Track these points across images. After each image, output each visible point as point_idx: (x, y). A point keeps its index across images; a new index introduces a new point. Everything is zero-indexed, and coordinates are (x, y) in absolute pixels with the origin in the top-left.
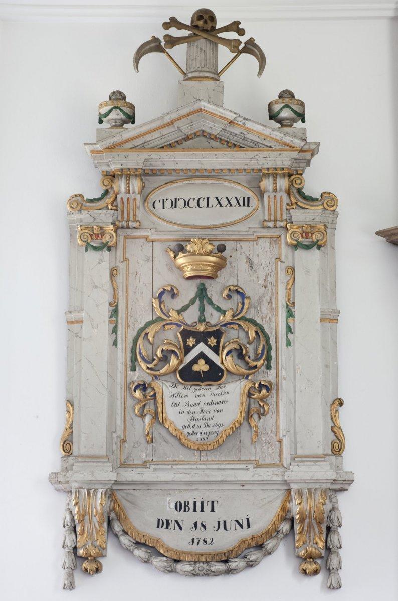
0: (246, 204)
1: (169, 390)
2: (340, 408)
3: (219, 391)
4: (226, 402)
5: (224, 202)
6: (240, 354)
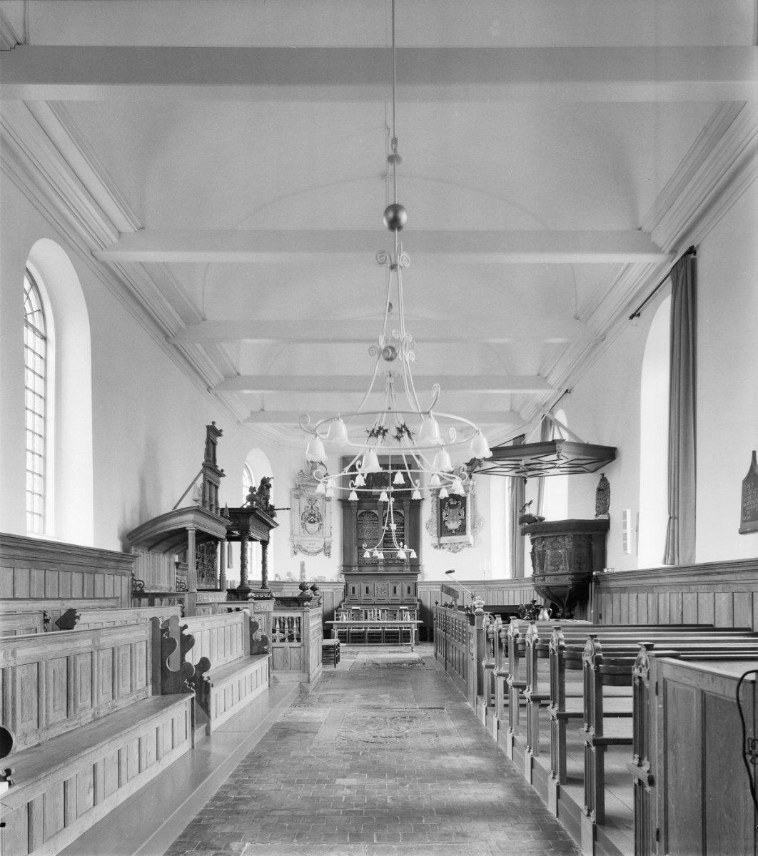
1: (307, 524)
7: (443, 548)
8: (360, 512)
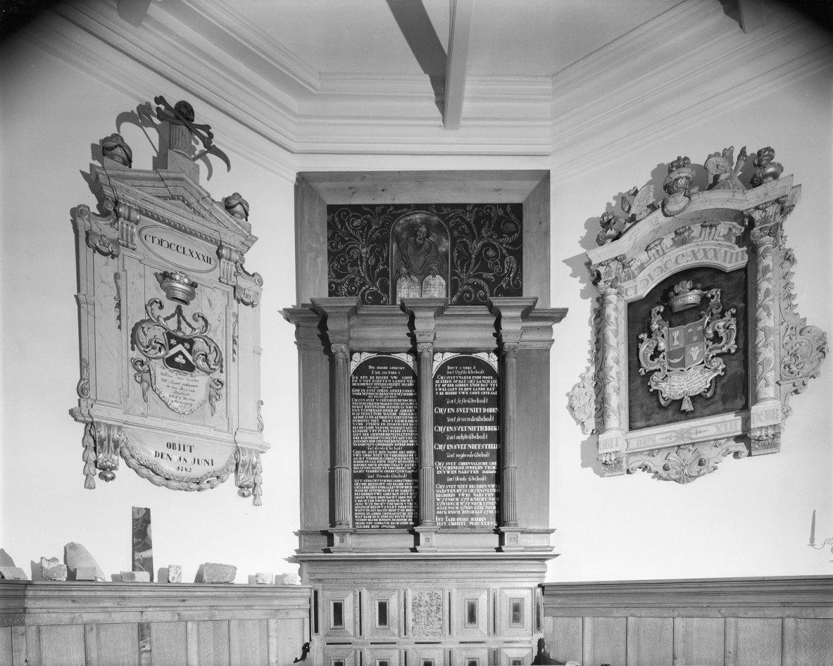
3: (192, 378)
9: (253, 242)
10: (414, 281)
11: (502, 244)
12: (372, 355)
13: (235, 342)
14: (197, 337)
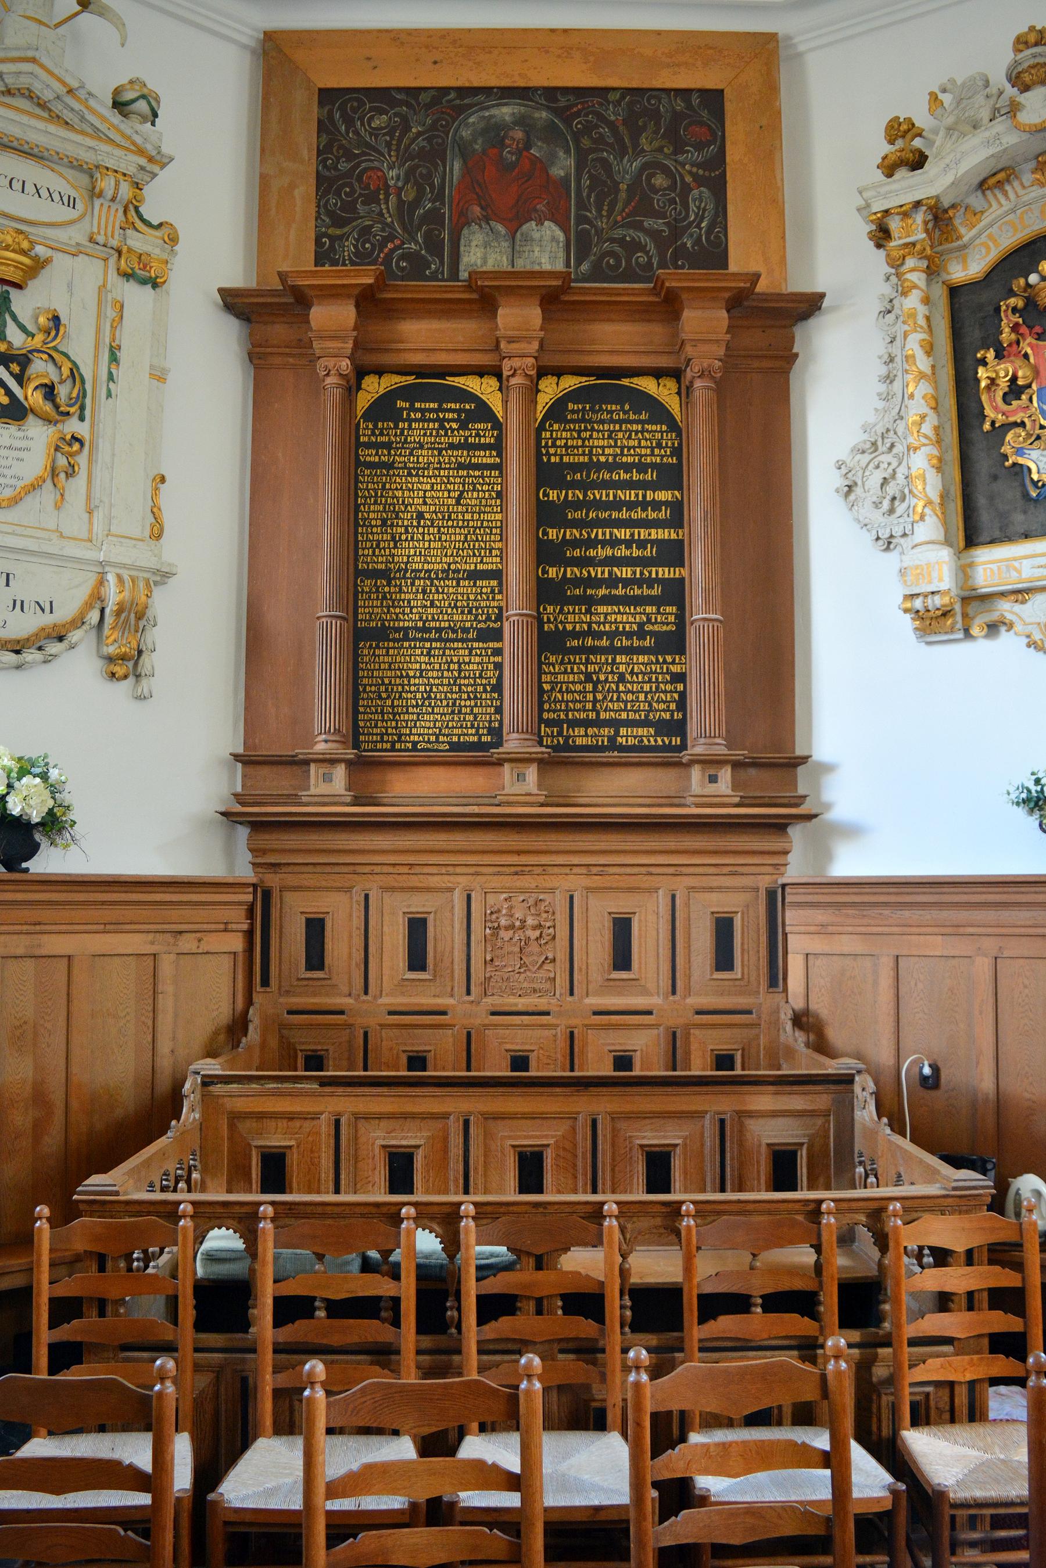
0: (71, 205)
2: (160, 485)
3: (20, 434)
4: (28, 449)
5: (44, 193)
6: (49, 391)
7: (993, 629)
8: (374, 387)
9: (163, 166)
10: (499, 233)
11: (683, 165)
12: (404, 378)
13: (114, 359)
14: (39, 351)
